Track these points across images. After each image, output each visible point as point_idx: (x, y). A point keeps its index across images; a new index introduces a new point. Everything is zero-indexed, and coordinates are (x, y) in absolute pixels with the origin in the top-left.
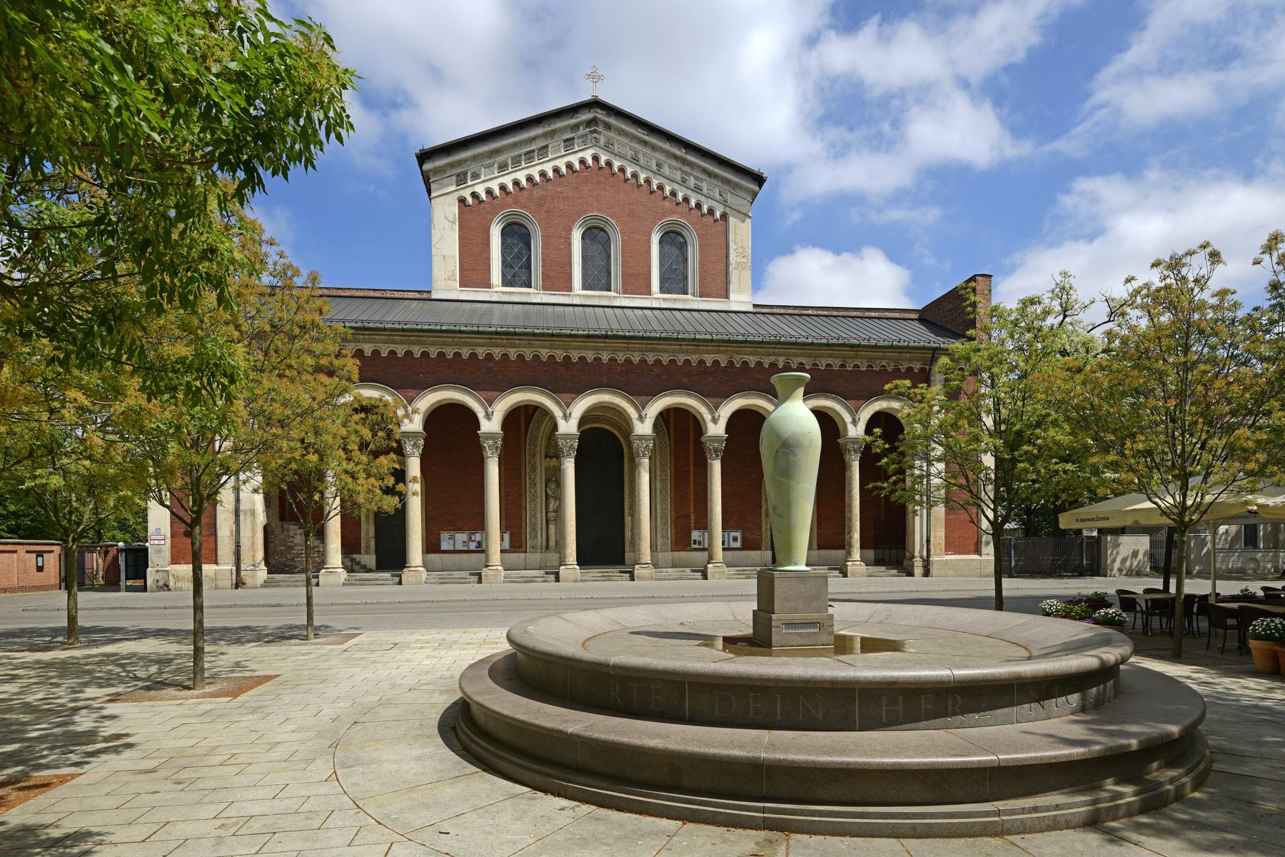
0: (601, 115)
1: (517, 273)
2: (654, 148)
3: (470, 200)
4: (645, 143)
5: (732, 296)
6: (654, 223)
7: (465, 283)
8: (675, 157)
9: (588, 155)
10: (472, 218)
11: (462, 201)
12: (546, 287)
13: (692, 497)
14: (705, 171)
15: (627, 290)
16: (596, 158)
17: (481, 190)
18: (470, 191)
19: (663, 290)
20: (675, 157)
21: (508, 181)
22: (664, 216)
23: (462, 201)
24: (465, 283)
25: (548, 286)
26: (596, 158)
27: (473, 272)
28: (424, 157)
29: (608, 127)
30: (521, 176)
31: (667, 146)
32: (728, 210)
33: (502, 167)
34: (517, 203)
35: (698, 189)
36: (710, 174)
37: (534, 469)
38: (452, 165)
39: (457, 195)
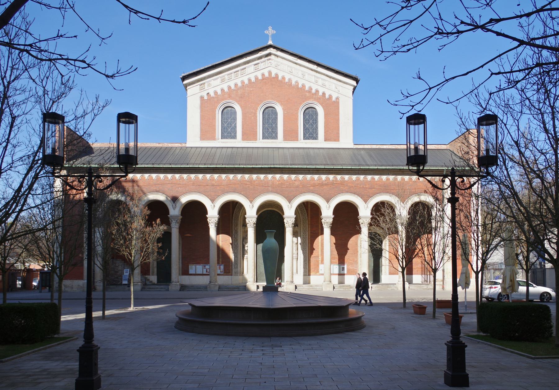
1: (229, 132)
3: (206, 98)
6: (301, 104)
10: (207, 104)
11: (202, 98)
12: (244, 139)
15: (286, 138)
16: (270, 73)
23: (202, 98)
25: (245, 137)
26: (270, 73)
27: (206, 132)
32: (339, 96)
34: (230, 97)
35: (323, 86)
38: (198, 81)
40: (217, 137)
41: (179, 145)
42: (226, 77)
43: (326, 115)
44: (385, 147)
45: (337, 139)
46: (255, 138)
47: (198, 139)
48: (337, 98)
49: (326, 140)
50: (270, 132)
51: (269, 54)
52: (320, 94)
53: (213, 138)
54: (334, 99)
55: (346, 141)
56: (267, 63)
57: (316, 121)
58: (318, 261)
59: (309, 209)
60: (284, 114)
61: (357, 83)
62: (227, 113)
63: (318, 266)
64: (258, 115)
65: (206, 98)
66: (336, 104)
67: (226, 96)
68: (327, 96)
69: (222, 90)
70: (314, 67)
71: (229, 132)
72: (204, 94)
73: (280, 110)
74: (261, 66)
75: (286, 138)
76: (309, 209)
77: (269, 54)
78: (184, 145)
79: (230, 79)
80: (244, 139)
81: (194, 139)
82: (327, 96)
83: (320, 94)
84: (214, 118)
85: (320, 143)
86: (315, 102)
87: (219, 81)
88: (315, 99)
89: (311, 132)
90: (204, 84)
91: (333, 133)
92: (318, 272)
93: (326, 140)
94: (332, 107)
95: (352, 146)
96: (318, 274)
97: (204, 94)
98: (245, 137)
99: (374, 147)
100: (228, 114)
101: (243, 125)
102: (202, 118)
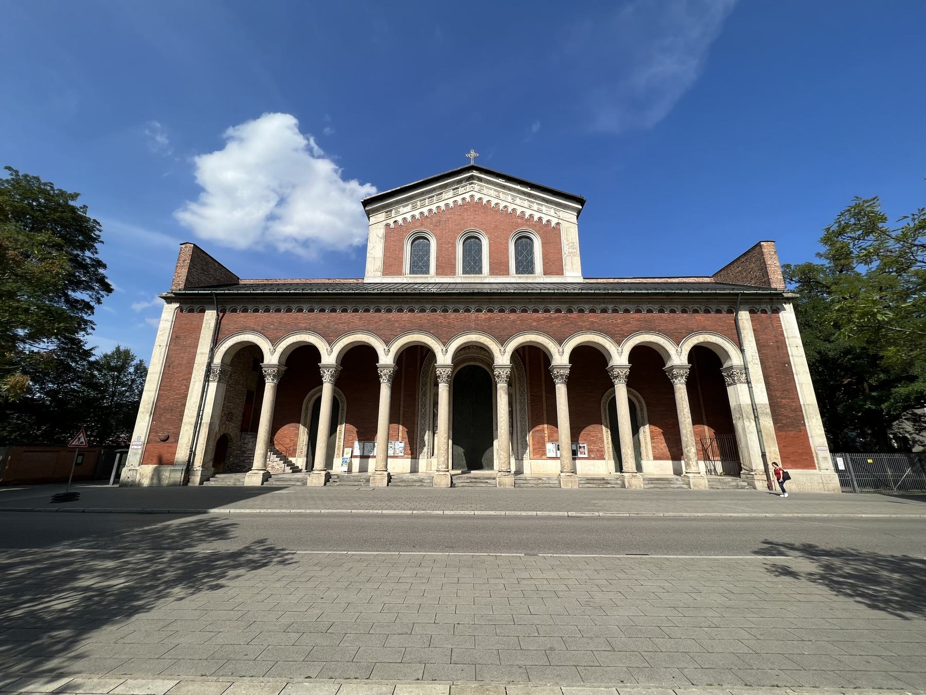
0: (475, 173)
2: (510, 189)
3: (392, 226)
4: (504, 187)
5: (566, 273)
7: (385, 273)
8: (524, 193)
9: (467, 196)
11: (388, 225)
12: (438, 274)
13: (545, 415)
14: (544, 200)
16: (472, 196)
17: (399, 219)
18: (394, 220)
19: (518, 271)
20: (524, 193)
21: (417, 213)
22: (518, 227)
23: (388, 225)
24: (385, 273)
25: (440, 271)
27: (391, 264)
28: (366, 203)
29: (480, 179)
30: (425, 210)
31: (518, 187)
32: (560, 221)
33: (414, 208)
35: (539, 211)
36: (547, 201)
37: (425, 394)
39: (385, 222)
40: (404, 271)
41: (355, 281)
42: (419, 203)
43: (544, 244)
44: (626, 281)
45: (560, 272)
46: (453, 272)
47: (379, 274)
48: (558, 224)
49: (546, 273)
50: (472, 265)
51: (472, 177)
52: (536, 218)
53: (399, 273)
54: (553, 224)
55: (573, 274)
56: (468, 188)
57: (531, 252)
58: (543, 438)
59: (527, 362)
60: (490, 244)
61: (582, 205)
62: (418, 245)
63: (544, 445)
64: (457, 245)
65: (392, 226)
66: (557, 230)
67: (418, 224)
68: (544, 222)
69: (413, 216)
70: (528, 190)
71: (419, 265)
72: (391, 222)
73: (485, 243)
74: (461, 190)
75: (493, 272)
76: (527, 362)
77: (472, 177)
78: (360, 281)
79: (423, 206)
80: (438, 274)
81: (374, 274)
82: (544, 222)
83: (536, 218)
84: (402, 249)
85: (539, 277)
86: (530, 230)
87: (409, 208)
88: (529, 226)
89: (525, 265)
90: (391, 211)
91: (554, 265)
92: (545, 454)
93: (546, 273)
94: (552, 235)
95: (581, 280)
96: (544, 457)
97: (391, 222)
98: (440, 271)
99: (611, 281)
100: (420, 240)
101: (437, 258)
102: (386, 249)
